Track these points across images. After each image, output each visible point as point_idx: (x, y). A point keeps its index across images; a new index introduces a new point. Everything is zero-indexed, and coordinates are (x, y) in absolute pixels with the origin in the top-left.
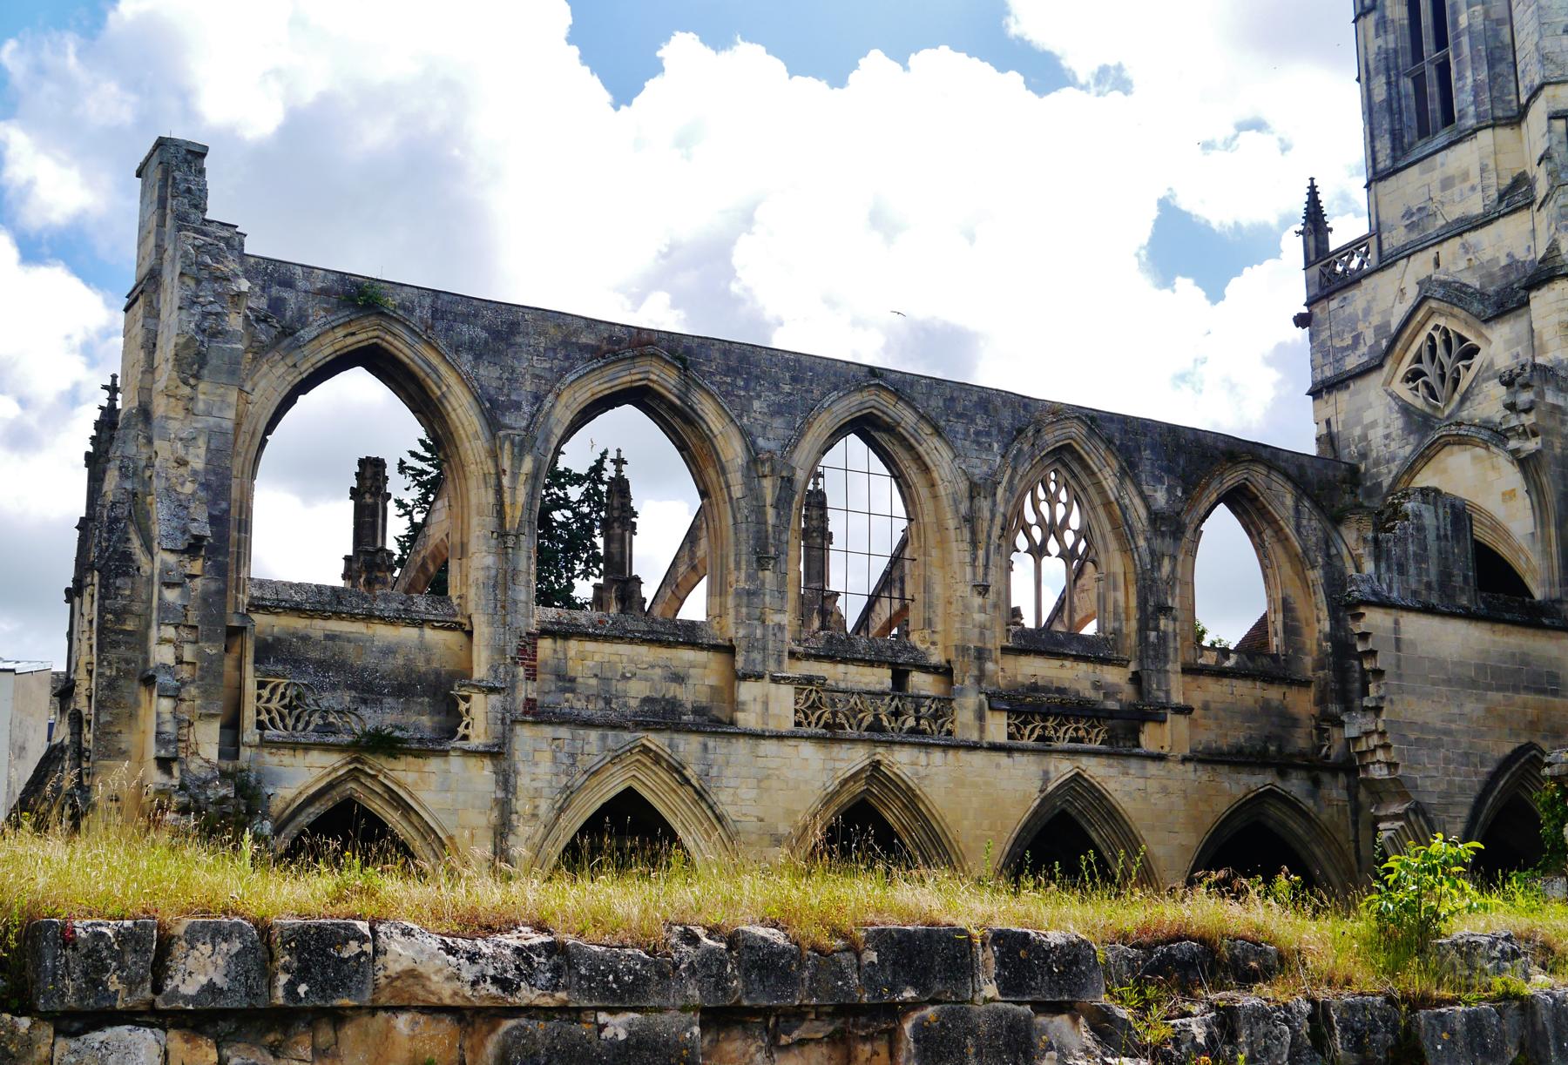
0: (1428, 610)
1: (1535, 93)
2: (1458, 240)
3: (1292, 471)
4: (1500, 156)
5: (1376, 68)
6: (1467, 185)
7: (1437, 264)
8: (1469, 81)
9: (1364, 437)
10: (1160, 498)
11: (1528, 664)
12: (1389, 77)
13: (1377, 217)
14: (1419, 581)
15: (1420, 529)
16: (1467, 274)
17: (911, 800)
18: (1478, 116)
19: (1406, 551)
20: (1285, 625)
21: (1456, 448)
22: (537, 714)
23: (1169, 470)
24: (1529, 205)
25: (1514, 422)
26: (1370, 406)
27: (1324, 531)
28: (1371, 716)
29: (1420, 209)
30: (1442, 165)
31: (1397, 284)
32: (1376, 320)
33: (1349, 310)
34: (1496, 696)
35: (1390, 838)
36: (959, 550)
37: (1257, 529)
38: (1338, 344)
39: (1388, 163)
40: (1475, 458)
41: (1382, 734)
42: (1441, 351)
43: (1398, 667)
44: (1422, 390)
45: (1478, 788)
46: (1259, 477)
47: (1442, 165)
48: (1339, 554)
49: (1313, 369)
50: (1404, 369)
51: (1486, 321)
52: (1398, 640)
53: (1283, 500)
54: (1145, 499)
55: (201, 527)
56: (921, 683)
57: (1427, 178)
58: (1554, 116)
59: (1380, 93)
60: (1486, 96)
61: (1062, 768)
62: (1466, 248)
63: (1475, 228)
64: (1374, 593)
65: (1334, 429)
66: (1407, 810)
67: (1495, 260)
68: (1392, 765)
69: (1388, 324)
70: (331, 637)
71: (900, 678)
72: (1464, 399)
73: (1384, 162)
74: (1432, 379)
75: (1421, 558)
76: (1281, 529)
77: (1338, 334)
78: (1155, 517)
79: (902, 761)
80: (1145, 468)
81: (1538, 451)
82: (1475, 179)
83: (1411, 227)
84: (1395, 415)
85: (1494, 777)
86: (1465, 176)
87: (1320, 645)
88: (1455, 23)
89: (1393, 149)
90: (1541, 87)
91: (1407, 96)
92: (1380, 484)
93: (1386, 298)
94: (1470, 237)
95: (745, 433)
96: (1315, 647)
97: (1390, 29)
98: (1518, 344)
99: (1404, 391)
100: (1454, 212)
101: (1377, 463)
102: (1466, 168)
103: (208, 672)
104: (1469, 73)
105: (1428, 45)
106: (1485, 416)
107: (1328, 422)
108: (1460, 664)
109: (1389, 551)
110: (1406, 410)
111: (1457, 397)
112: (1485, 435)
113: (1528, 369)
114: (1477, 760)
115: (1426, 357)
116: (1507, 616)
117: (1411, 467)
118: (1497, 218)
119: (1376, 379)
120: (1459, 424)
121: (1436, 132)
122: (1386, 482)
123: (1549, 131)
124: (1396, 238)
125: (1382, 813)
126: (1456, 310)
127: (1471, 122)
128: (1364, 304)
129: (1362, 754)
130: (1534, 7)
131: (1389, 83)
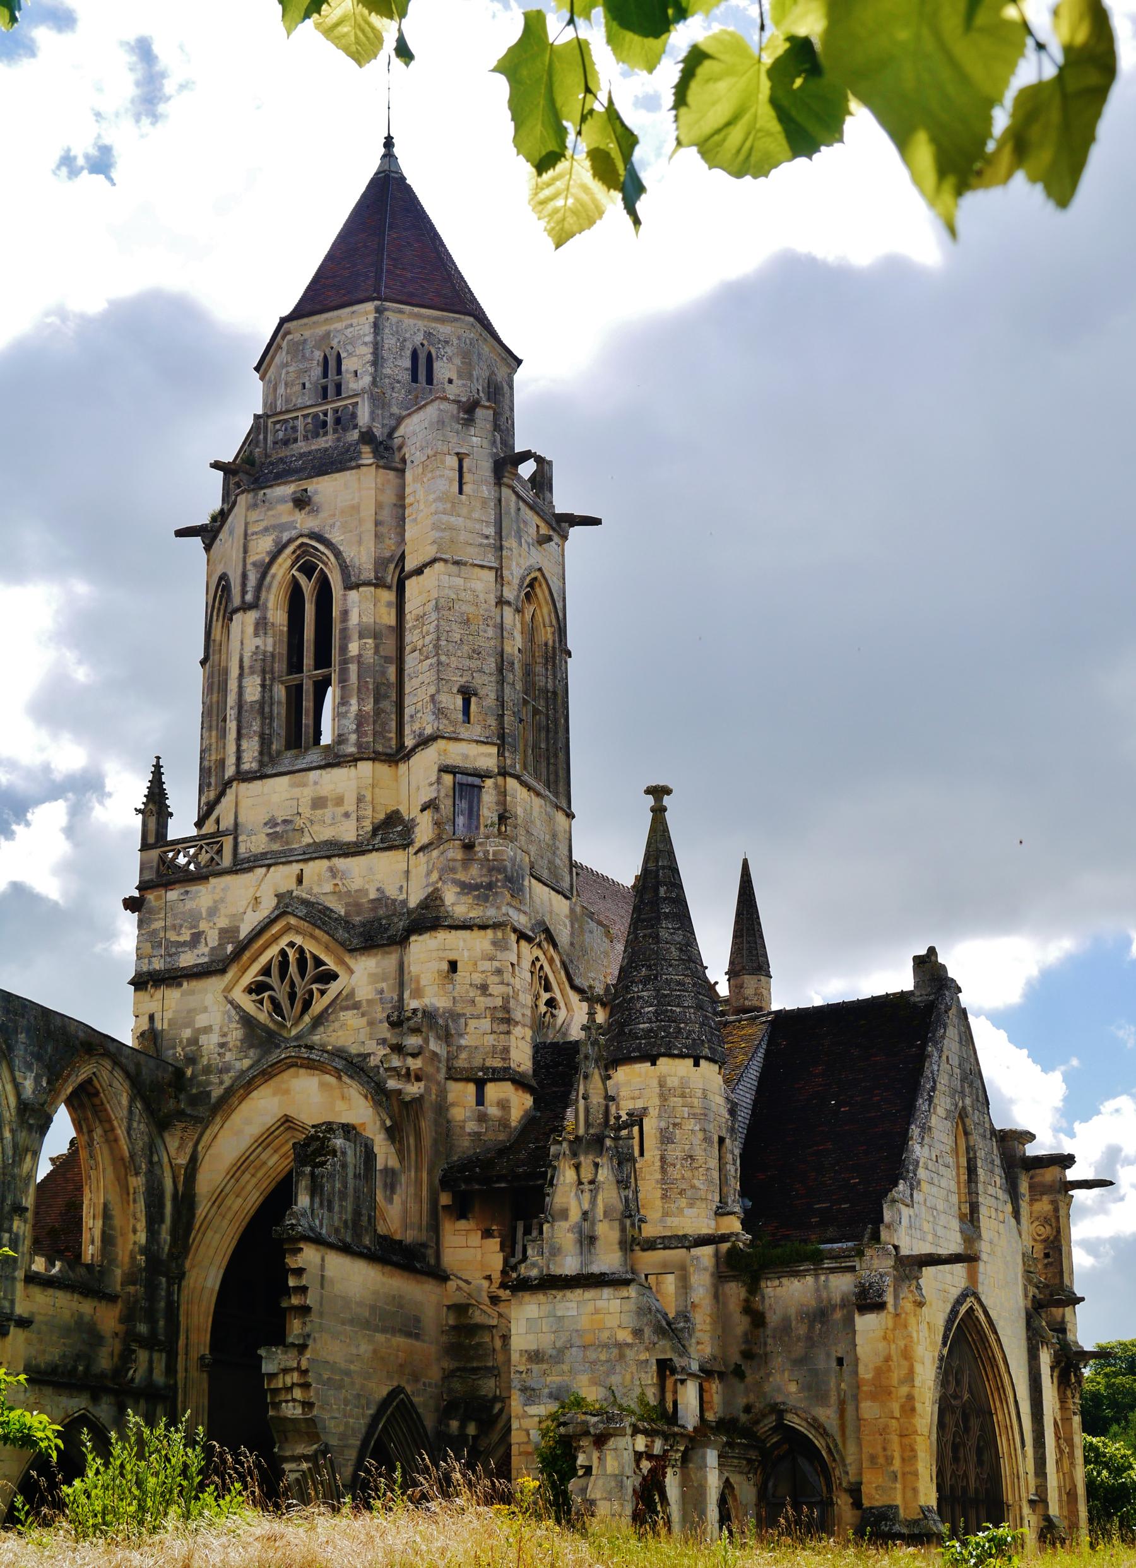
0: (345, 1249)
1: (425, 742)
2: (325, 864)
3: (131, 1068)
4: (377, 790)
5: (251, 667)
6: (340, 810)
7: (300, 880)
8: (354, 708)
9: (193, 1041)
10: (28, 1085)
11: (401, 1306)
12: (264, 680)
13: (236, 818)
14: (340, 1218)
15: (344, 1166)
16: (330, 898)
18: (359, 745)
19: (333, 1187)
20: (103, 1232)
21: (302, 1071)
23: (39, 1057)
24: (405, 847)
25: (396, 1062)
26: (205, 1010)
27: (150, 1135)
28: (293, 1353)
29: (285, 821)
30: (316, 783)
31: (252, 891)
32: (223, 922)
33: (190, 905)
34: (380, 1337)
35: (297, 1479)
37: (88, 1126)
38: (173, 937)
39: (255, 766)
40: (322, 1085)
41: (304, 1373)
42: (293, 969)
43: (321, 1305)
44: (267, 1003)
45: (363, 1430)
47: (316, 783)
48: (160, 1162)
49: (139, 957)
50: (250, 976)
51: (351, 951)
52: (322, 1276)
53: (119, 1098)
54: (17, 1086)
57: (297, 792)
58: (444, 769)
59: (253, 693)
60: (369, 728)
63: (346, 855)
64: (312, 1229)
65: (158, 1025)
66: (316, 1451)
67: (362, 892)
68: (307, 1405)
69: (236, 930)
72: (319, 1021)
73: (250, 763)
74: (282, 997)
75: (343, 1196)
76: (113, 1129)
77: (174, 927)
78: (24, 1108)
80: (20, 1052)
81: (422, 1096)
82: (350, 805)
83: (273, 837)
84: (234, 1025)
85: (375, 1419)
86: (339, 801)
87: (133, 1258)
88: (344, 649)
89: (261, 753)
90: (433, 738)
91: (279, 703)
92: (209, 1094)
93: (239, 901)
94: (340, 863)
96: (127, 1259)
97: (270, 632)
98: (384, 980)
99: (247, 1003)
100: (324, 834)
101: (207, 1070)
102: (337, 795)
104: (354, 701)
105: (308, 660)
106: (339, 1044)
107: (152, 1018)
108: (360, 1304)
109: (322, 1187)
110: (247, 1021)
111: (307, 1019)
112: (339, 1064)
113: (420, 1015)
114: (363, 1401)
115: (275, 971)
116: (395, 1259)
117: (249, 1083)
118: (370, 851)
119: (214, 986)
120: (310, 1048)
121: (307, 749)
122: (216, 1093)
123: (439, 781)
124: (254, 843)
125: (288, 1454)
126: (317, 932)
127: (351, 749)
128: (210, 903)
129: (276, 1391)
130: (434, 660)
131: (263, 686)
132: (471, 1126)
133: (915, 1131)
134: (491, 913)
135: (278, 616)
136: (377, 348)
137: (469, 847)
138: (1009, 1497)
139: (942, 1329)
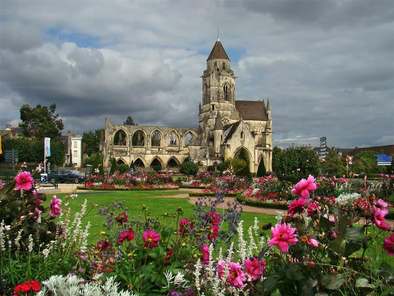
17: (160, 158)
22: (132, 153)
36: (164, 139)
46: (191, 131)
56: (160, 149)
61: (172, 155)
71: (159, 149)
79: (159, 155)
93: (203, 115)
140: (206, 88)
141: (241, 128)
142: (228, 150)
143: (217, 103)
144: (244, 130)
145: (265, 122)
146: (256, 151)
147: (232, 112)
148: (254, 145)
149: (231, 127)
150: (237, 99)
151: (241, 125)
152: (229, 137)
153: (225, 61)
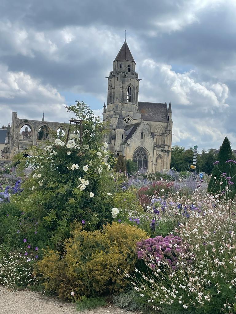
55: (17, 137)
62: (111, 112)
70: (24, 142)
93: (107, 114)
95: (52, 129)
103: (17, 145)
124: (108, 110)
132: (114, 133)
133: (133, 134)
134: (115, 117)
135: (110, 90)
136: (117, 65)
137: (114, 112)
138: (149, 160)
139: (135, 149)
140: (111, 89)
141: (141, 129)
142: (128, 149)
143: (120, 104)
144: (144, 131)
145: (166, 124)
146: (155, 151)
147: (134, 113)
148: (153, 146)
149: (133, 127)
150: (139, 101)
151: (141, 126)
152: (129, 136)
153: (131, 64)
